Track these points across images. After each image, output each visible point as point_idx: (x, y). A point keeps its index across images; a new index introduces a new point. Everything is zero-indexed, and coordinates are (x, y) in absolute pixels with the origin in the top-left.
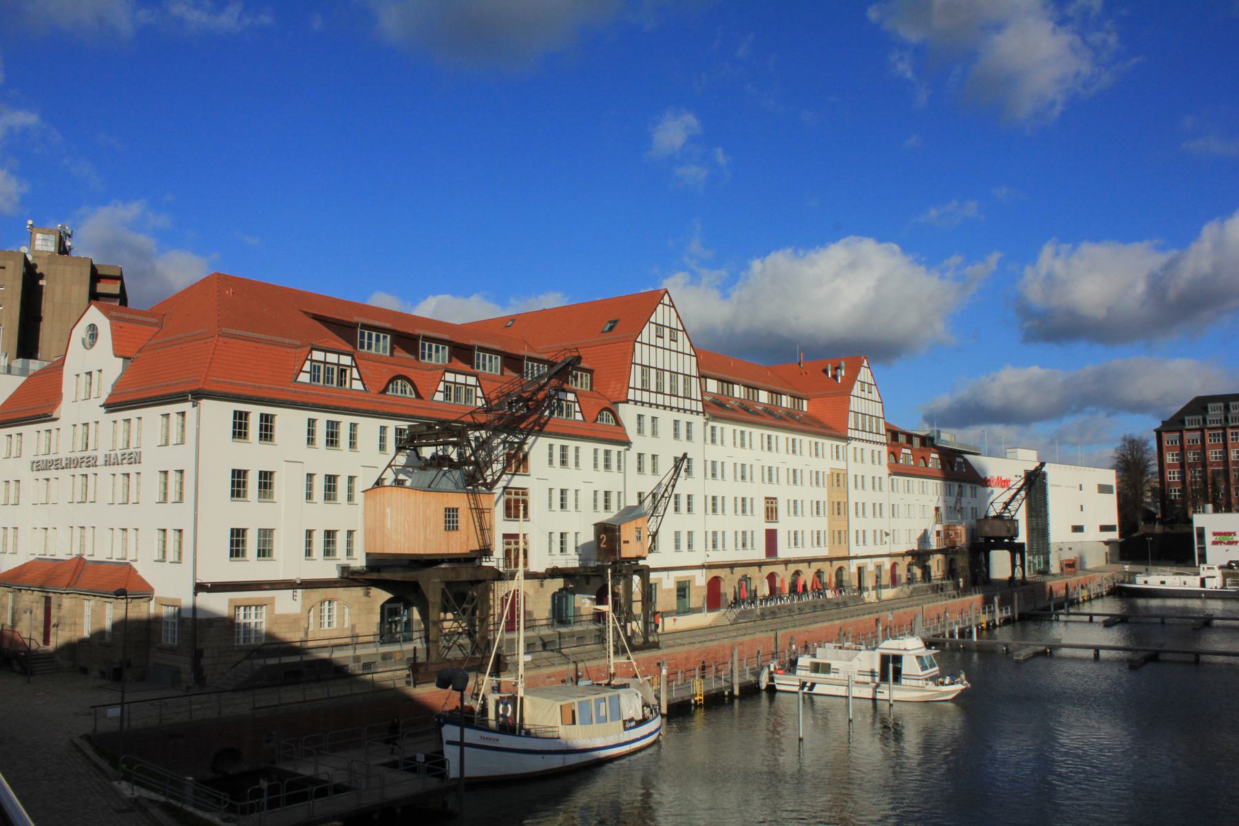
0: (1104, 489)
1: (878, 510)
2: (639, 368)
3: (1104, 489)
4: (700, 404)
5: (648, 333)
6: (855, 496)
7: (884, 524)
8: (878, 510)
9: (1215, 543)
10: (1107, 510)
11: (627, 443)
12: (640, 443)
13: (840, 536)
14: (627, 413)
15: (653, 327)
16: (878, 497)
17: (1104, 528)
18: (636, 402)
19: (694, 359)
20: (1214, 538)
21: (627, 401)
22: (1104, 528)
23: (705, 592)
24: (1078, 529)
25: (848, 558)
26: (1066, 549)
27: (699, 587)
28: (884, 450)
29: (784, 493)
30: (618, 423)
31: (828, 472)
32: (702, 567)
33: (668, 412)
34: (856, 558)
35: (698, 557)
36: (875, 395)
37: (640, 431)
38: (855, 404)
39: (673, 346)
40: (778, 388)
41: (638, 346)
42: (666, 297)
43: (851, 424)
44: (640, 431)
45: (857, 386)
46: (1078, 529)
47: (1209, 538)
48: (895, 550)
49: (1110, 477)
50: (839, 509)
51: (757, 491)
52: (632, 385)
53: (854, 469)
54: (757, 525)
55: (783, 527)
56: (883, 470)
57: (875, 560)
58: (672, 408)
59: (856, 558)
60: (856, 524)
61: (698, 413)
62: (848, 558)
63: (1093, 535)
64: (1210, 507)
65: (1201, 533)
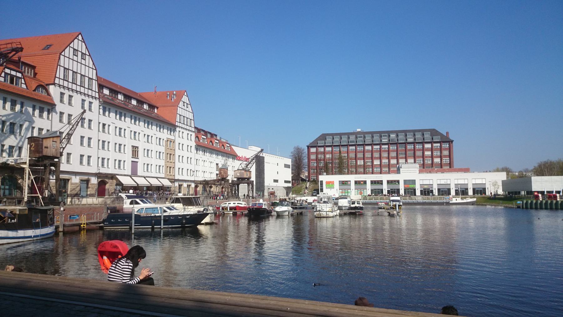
0: (287, 166)
2: (62, 69)
3: (287, 166)
4: (97, 94)
5: (68, 52)
10: (288, 175)
12: (59, 107)
15: (72, 50)
16: (190, 155)
17: (286, 182)
19: (95, 71)
21: (54, 84)
22: (286, 182)
23: (96, 187)
24: (276, 181)
26: (271, 189)
27: (93, 184)
28: (194, 134)
29: (142, 145)
30: (49, 94)
31: (166, 139)
35: (94, 170)
36: (190, 109)
37: (62, 101)
38: (180, 111)
39: (83, 62)
41: (62, 57)
42: (80, 36)
43: (178, 120)
44: (62, 101)
45: (181, 103)
46: (276, 181)
48: (197, 179)
49: (289, 162)
51: (129, 143)
52: (57, 76)
56: (193, 144)
58: (81, 93)
60: (178, 165)
61: (96, 98)
64: (325, 173)
65: (322, 182)
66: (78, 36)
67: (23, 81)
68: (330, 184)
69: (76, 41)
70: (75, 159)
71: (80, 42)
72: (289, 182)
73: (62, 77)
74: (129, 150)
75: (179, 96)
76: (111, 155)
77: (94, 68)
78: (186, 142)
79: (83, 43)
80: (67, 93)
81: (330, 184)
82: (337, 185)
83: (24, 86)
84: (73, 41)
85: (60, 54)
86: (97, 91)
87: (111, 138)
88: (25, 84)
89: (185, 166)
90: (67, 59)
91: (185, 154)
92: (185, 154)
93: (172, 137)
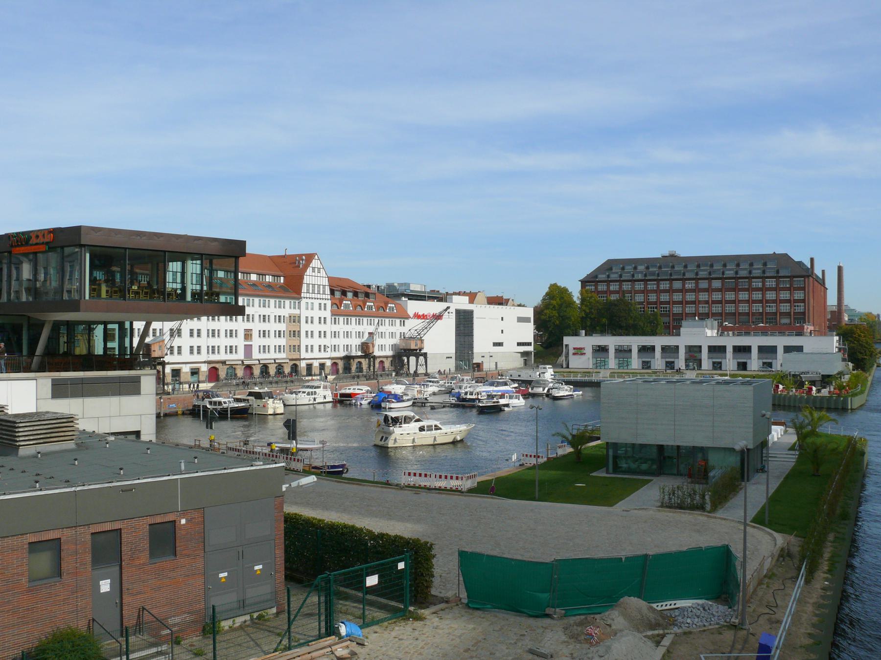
0: (521, 320)
1: (322, 334)
3: (521, 320)
6: (304, 327)
7: (328, 341)
8: (322, 334)
9: (574, 354)
10: (528, 332)
20: (574, 351)
25: (300, 360)
31: (287, 316)
32: (205, 362)
34: (304, 359)
40: (264, 272)
47: (571, 351)
50: (296, 334)
53: (304, 313)
54: (239, 342)
55: (257, 342)
56: (327, 314)
59: (304, 359)
60: (304, 341)
62: (300, 360)
63: (511, 347)
68: (579, 351)
70: (186, 350)
72: (529, 344)
74: (241, 334)
75: (310, 257)
78: (316, 314)
81: (579, 351)
82: (589, 351)
89: (316, 342)
91: (316, 327)
92: (316, 327)
93: (297, 312)
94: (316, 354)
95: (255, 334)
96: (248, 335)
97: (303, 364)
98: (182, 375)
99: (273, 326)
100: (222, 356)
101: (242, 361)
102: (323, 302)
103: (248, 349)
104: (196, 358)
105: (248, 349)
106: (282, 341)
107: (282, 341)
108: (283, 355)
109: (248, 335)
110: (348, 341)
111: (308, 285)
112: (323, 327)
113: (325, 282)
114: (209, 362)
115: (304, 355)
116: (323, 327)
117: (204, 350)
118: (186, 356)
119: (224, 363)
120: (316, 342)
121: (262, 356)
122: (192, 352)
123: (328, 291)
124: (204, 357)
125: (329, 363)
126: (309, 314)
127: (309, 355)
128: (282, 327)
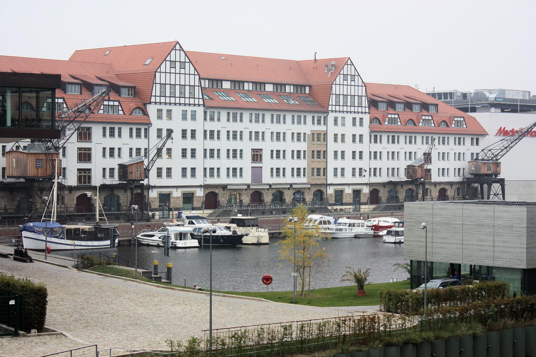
1: (357, 155)
6: (332, 147)
7: (365, 163)
8: (357, 155)
11: (150, 124)
13: (322, 172)
14: (152, 110)
18: (156, 103)
21: (150, 103)
25: (327, 185)
29: (267, 146)
30: (145, 113)
32: (200, 186)
33: (178, 107)
50: (321, 154)
51: (247, 146)
56: (365, 131)
57: (351, 187)
60: (332, 164)
62: (327, 185)
66: (175, 46)
67: (120, 108)
69: (173, 52)
70: (177, 173)
71: (178, 52)
73: (158, 94)
74: (248, 155)
76: (224, 163)
77: (196, 73)
79: (182, 52)
80: (165, 108)
83: (121, 112)
84: (170, 53)
85: (156, 72)
86: (201, 97)
87: (224, 144)
88: (122, 110)
89: (349, 164)
90: (163, 75)
93: (322, 128)
94: (348, 178)
95: (266, 155)
96: (257, 156)
97: (331, 191)
98: (172, 200)
99: (289, 146)
100: (223, 180)
101: (249, 186)
102: (358, 116)
103: (257, 173)
104: (189, 181)
105: (257, 173)
106: (302, 164)
107: (302, 164)
108: (303, 180)
109: (257, 156)
110: (393, 164)
111: (337, 96)
112: (358, 147)
113: (362, 91)
114: (206, 187)
115: (331, 179)
116: (358, 147)
117: (199, 173)
118: (177, 179)
119: (224, 187)
120: (349, 164)
121: (275, 180)
122: (184, 175)
123: (365, 102)
124: (199, 180)
125: (366, 190)
126: (339, 130)
127: (339, 180)
128: (303, 146)
